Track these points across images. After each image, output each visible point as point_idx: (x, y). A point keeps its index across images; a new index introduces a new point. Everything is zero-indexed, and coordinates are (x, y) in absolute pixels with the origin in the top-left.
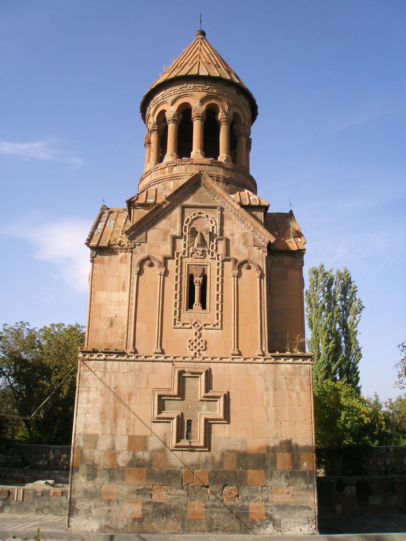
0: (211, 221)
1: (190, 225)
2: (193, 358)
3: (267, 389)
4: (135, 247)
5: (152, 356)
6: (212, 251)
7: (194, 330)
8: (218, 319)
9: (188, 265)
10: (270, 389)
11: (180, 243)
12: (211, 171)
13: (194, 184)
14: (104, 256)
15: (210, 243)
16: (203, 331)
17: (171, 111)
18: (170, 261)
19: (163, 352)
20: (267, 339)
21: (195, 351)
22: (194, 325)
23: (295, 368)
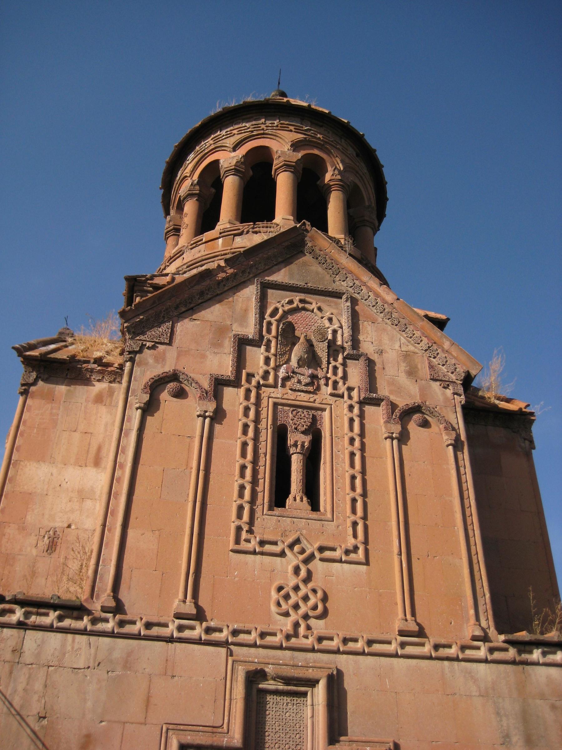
0: (330, 320)
1: (279, 321)
4: (140, 351)
6: (333, 378)
7: (293, 559)
8: (355, 536)
9: (275, 405)
10: (514, 739)
11: (256, 358)
14: (57, 383)
15: (329, 363)
16: (317, 566)
19: (200, 615)
20: (488, 595)
21: (294, 617)
22: (291, 546)
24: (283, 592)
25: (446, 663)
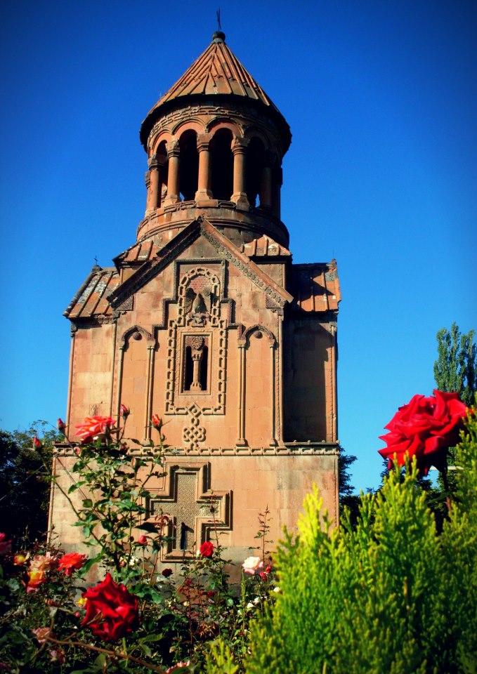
0: (214, 279)
1: (187, 286)
2: (189, 451)
3: (280, 487)
4: (119, 317)
5: (139, 450)
6: (213, 317)
7: (191, 416)
8: (220, 402)
9: (185, 336)
11: (174, 309)
12: (218, 216)
13: (192, 233)
15: (211, 307)
16: (202, 417)
17: (172, 141)
18: (161, 333)
20: (281, 424)
21: (191, 442)
22: (191, 410)
23: (317, 461)
24: (187, 431)
25: (257, 457)
